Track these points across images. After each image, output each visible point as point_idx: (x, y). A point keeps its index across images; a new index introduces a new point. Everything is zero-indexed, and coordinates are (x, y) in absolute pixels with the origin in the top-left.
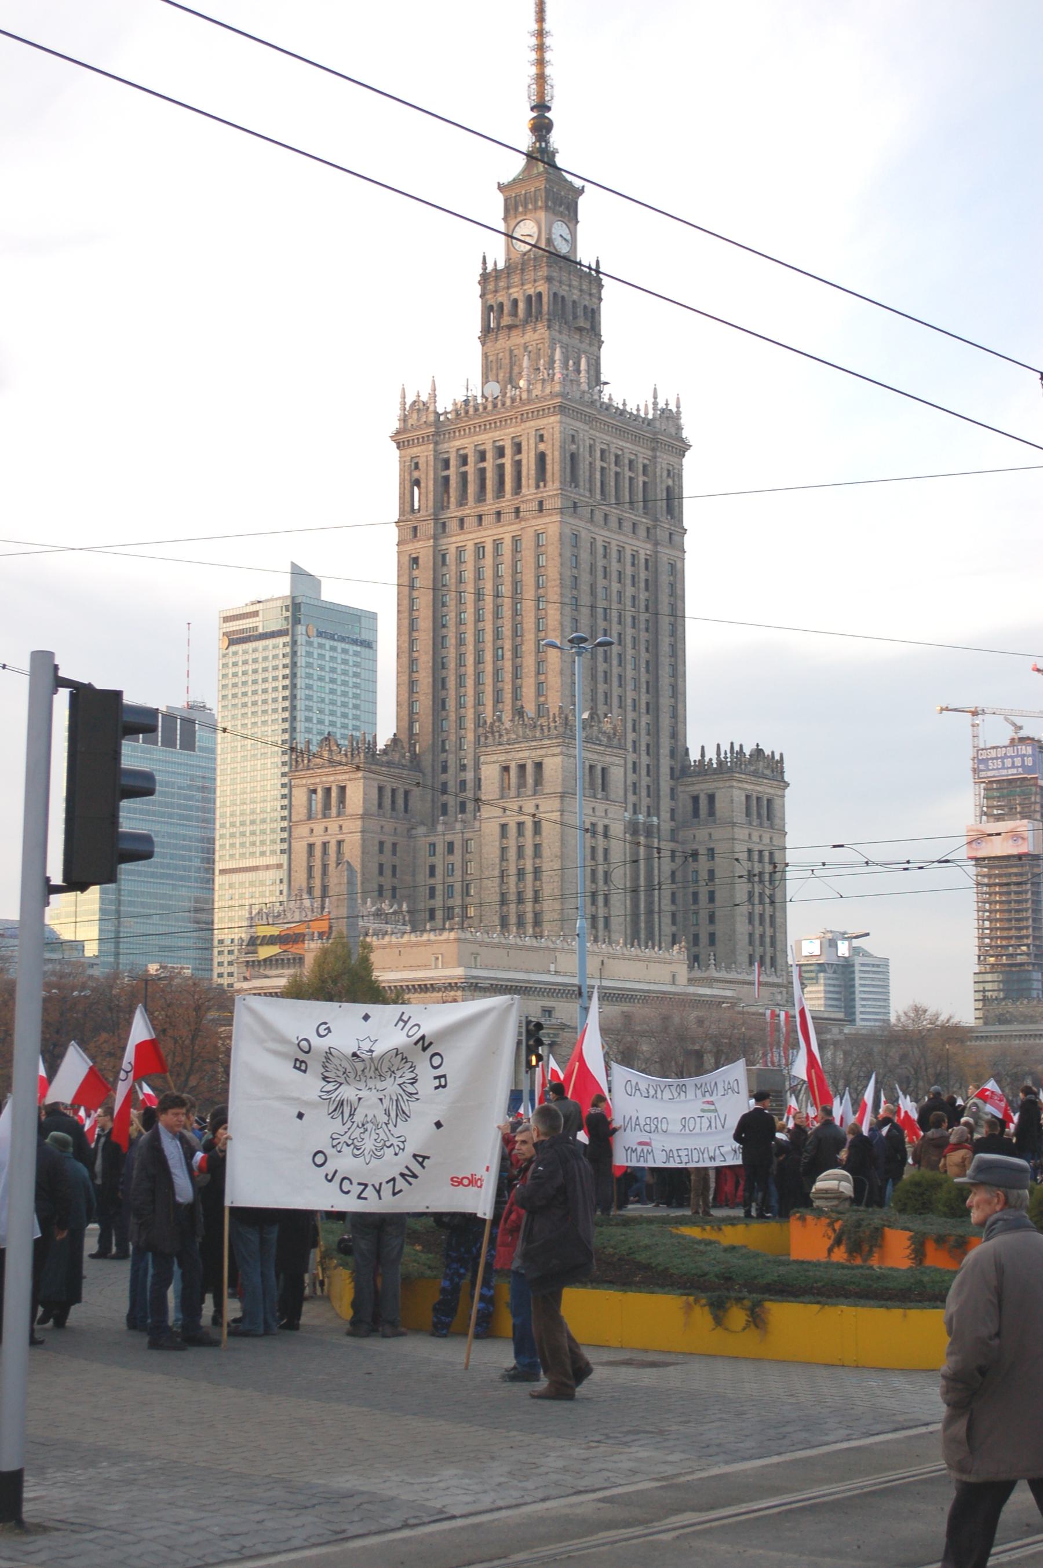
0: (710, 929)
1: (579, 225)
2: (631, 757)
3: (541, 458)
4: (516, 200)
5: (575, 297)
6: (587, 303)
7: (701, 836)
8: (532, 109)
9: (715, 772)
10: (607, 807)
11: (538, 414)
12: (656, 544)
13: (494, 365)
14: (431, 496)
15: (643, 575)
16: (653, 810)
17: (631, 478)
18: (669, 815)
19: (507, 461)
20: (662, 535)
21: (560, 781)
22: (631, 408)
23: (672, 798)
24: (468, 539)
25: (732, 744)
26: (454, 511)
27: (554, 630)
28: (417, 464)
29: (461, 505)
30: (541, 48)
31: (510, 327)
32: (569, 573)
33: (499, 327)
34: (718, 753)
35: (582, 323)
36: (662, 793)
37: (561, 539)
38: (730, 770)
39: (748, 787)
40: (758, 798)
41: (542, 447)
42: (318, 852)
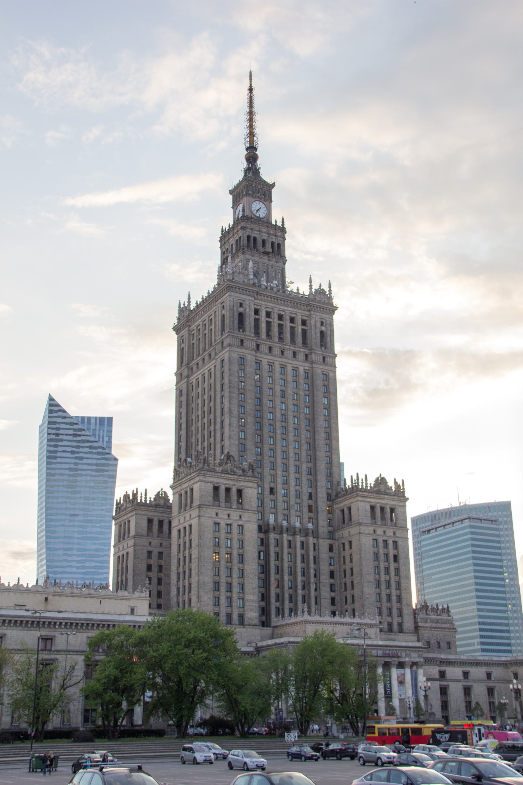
1: (272, 203)
5: (264, 237)
10: (241, 514)
12: (312, 363)
16: (315, 520)
17: (291, 327)
21: (199, 498)
25: (357, 474)
27: (227, 414)
30: (251, 120)
36: (319, 509)
39: (372, 500)
40: (382, 509)
41: (223, 312)
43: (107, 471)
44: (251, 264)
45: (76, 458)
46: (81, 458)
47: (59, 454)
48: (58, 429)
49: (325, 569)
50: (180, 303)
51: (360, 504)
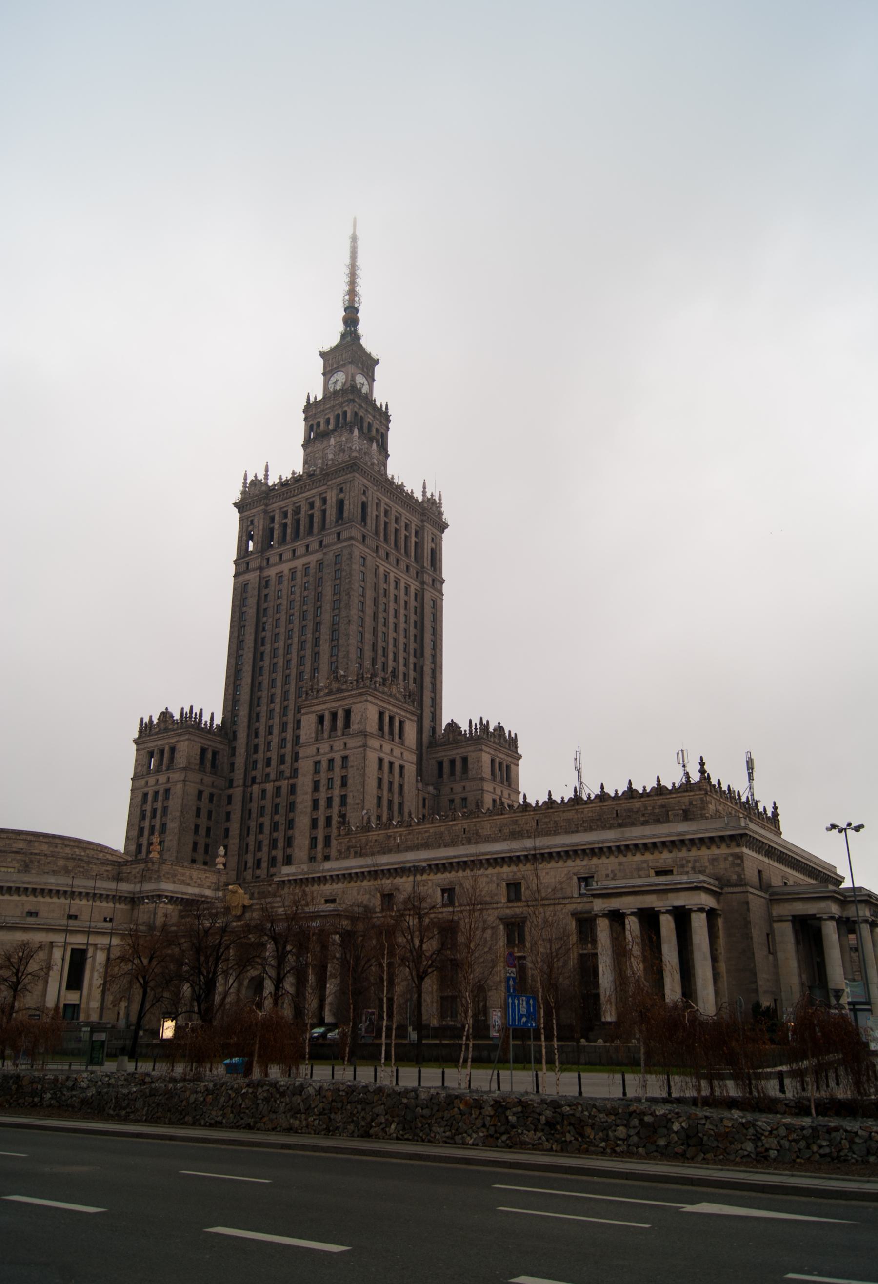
1: (375, 383)
3: (341, 504)
4: (333, 360)
5: (369, 420)
8: (345, 310)
15: (413, 603)
17: (406, 537)
20: (428, 579)
22: (408, 488)
24: (285, 568)
28: (252, 522)
33: (315, 438)
41: (341, 496)
42: (150, 798)
50: (246, 475)
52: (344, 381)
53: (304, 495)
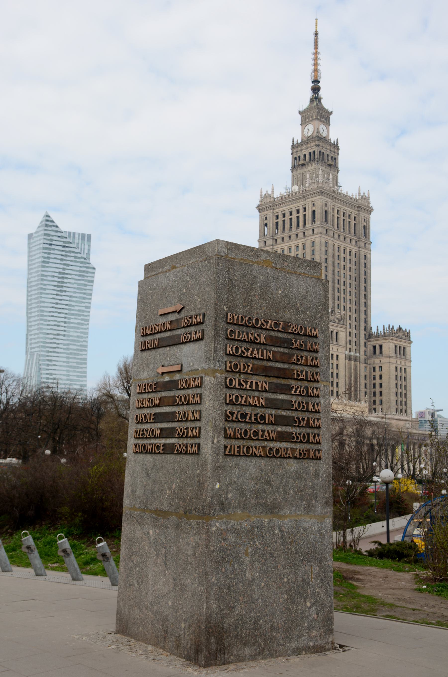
0: (380, 398)
2: (348, 330)
3: (314, 212)
5: (328, 153)
6: (333, 155)
7: (377, 361)
8: (313, 82)
9: (382, 336)
11: (313, 194)
12: (359, 247)
13: (296, 180)
14: (271, 230)
15: (354, 259)
17: (349, 222)
18: (364, 353)
19: (301, 215)
20: (361, 244)
22: (350, 194)
23: (365, 346)
25: (389, 325)
26: (280, 235)
28: (266, 218)
29: (283, 232)
30: (316, 59)
31: (303, 165)
32: (324, 257)
34: (384, 329)
35: (330, 162)
36: (361, 344)
37: (320, 244)
38: (389, 335)
40: (400, 347)
41: (314, 208)
43: (87, 277)
44: (331, 177)
45: (64, 264)
46: (68, 265)
47: (51, 260)
48: (52, 240)
49: (363, 382)
50: (261, 190)
51: (391, 344)
52: (313, 130)
53: (294, 205)
